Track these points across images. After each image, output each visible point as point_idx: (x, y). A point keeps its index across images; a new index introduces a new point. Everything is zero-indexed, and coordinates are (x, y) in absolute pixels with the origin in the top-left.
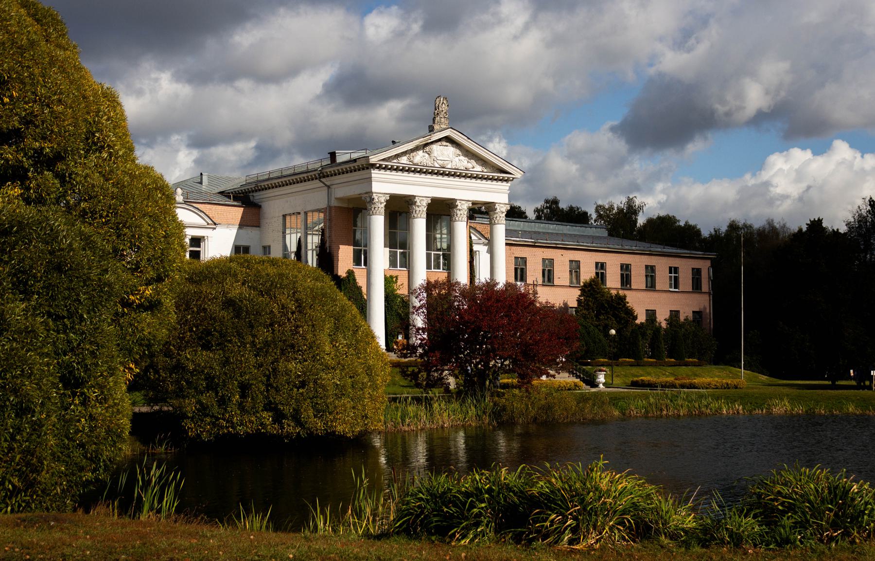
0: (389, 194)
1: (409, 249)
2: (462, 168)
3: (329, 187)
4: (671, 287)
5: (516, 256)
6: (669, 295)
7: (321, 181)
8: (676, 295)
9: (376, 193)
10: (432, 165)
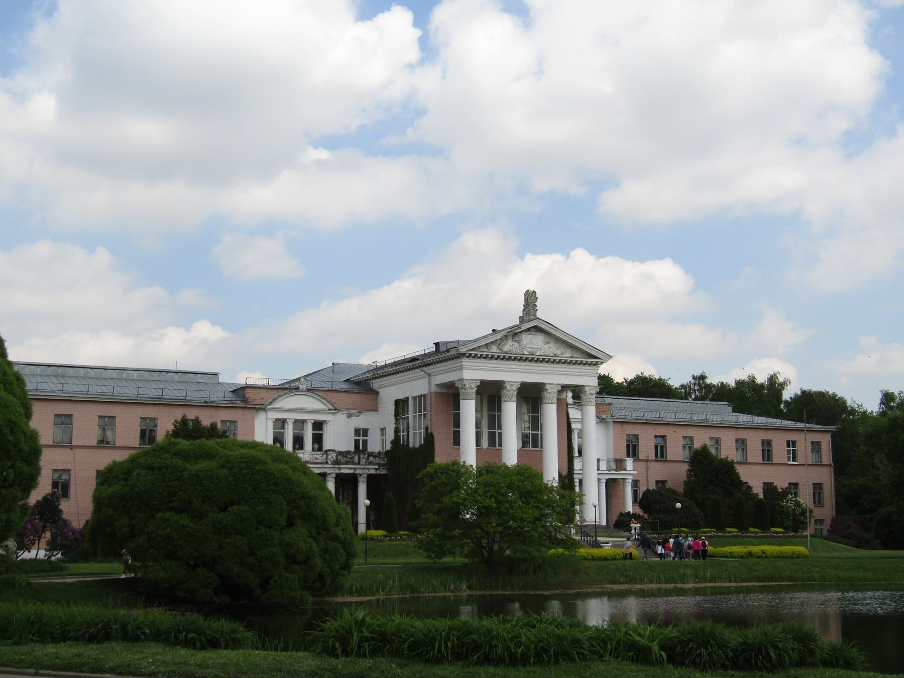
0: (479, 380)
1: (542, 430)
2: (551, 354)
3: (430, 375)
4: (789, 459)
5: (628, 433)
6: (790, 468)
7: (422, 370)
8: (794, 468)
9: (466, 379)
10: (522, 353)
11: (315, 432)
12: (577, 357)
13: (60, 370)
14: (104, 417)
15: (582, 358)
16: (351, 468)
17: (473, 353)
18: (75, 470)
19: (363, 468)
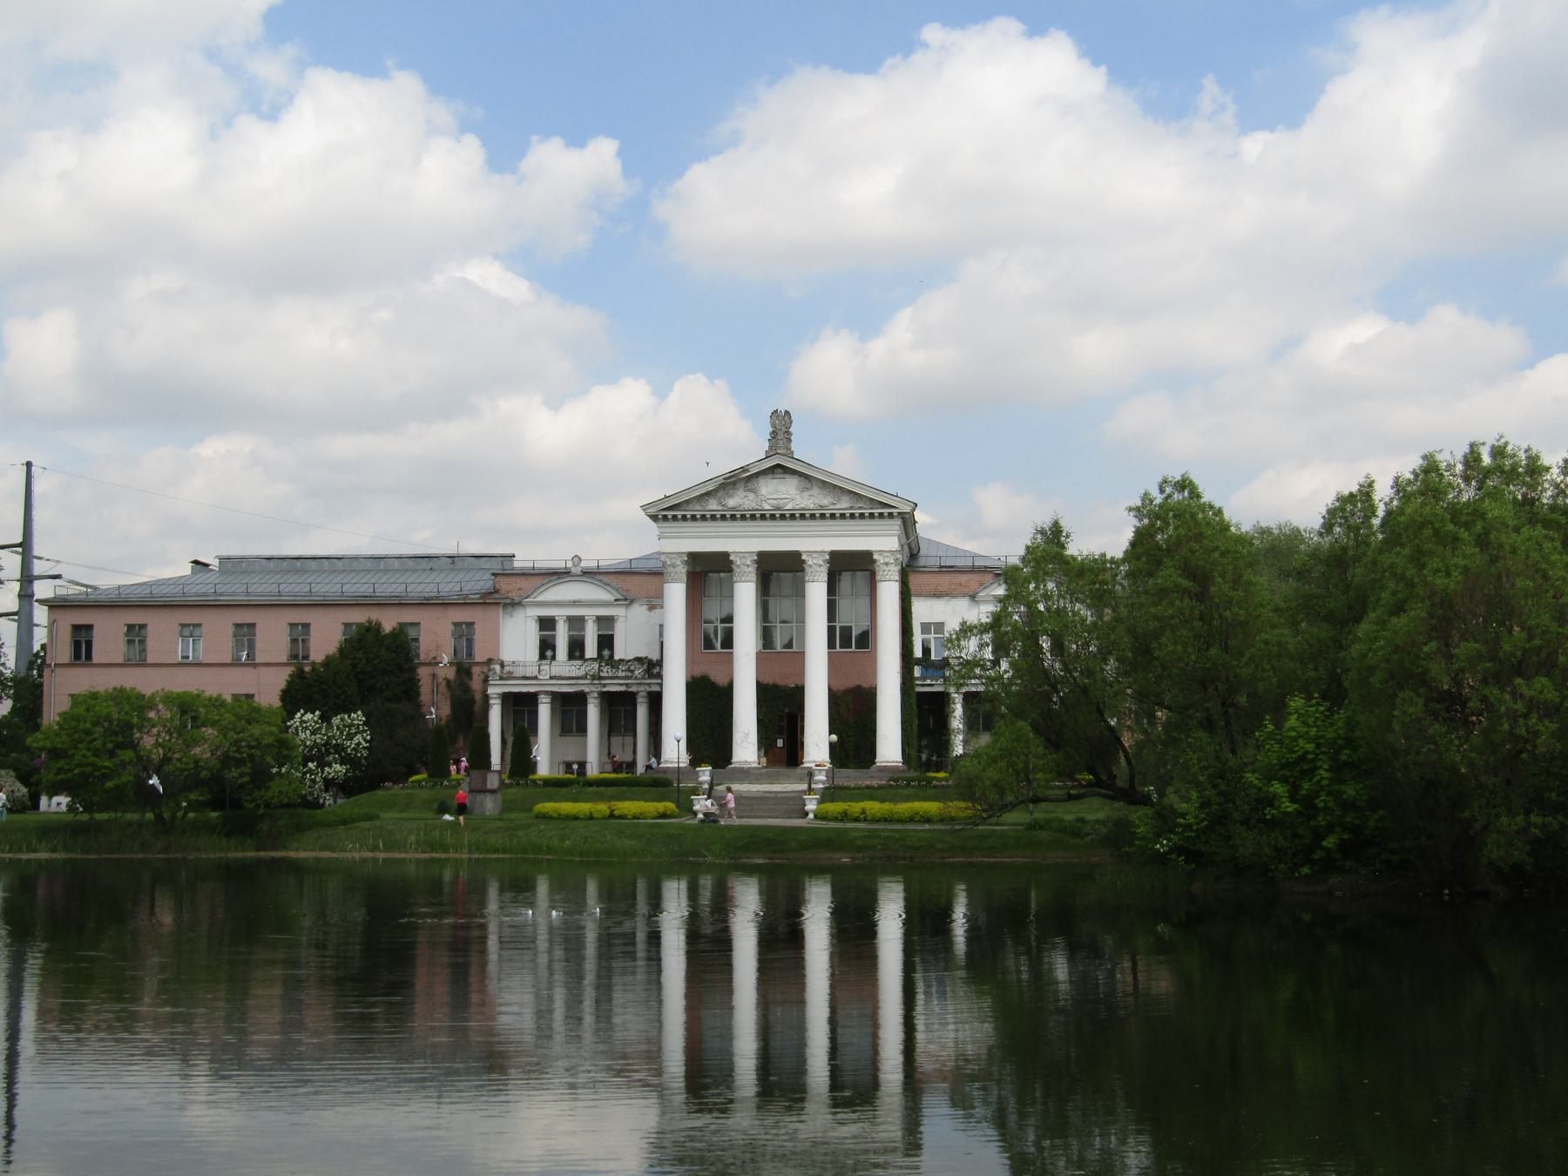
11: (600, 633)
12: (860, 508)
13: (299, 563)
14: (297, 625)
15: (872, 509)
16: (621, 684)
17: (670, 514)
18: (259, 694)
19: (641, 684)
